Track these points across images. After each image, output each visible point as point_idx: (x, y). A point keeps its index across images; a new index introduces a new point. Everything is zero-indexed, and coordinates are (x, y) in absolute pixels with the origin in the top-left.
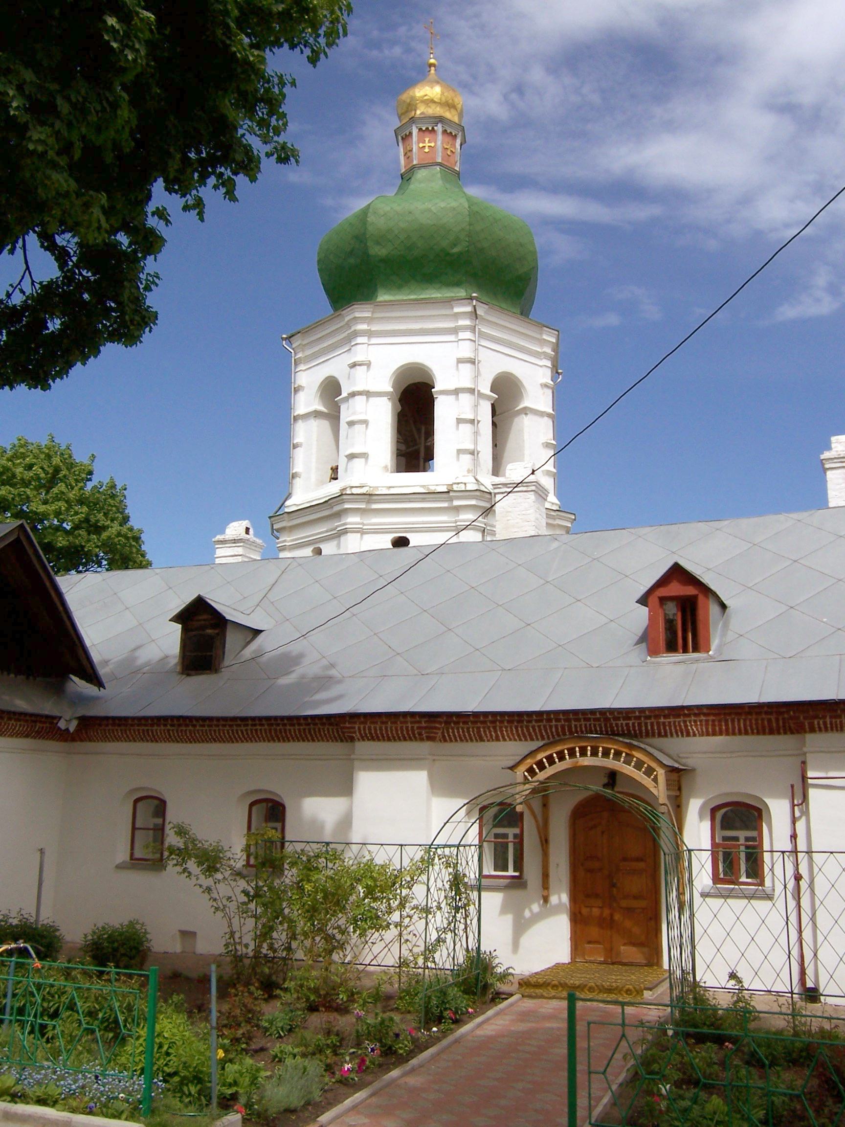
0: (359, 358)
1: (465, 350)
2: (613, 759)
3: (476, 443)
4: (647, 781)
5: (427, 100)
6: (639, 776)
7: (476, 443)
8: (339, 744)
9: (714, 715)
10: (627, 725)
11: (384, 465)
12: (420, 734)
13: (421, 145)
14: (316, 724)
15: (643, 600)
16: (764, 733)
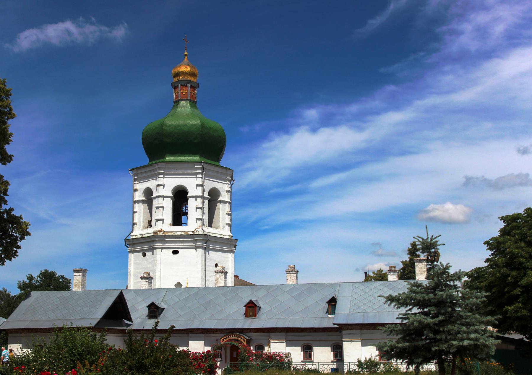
1: (199, 181)
4: (243, 341)
5: (185, 72)
6: (242, 340)
11: (169, 223)
13: (182, 91)
15: (244, 307)
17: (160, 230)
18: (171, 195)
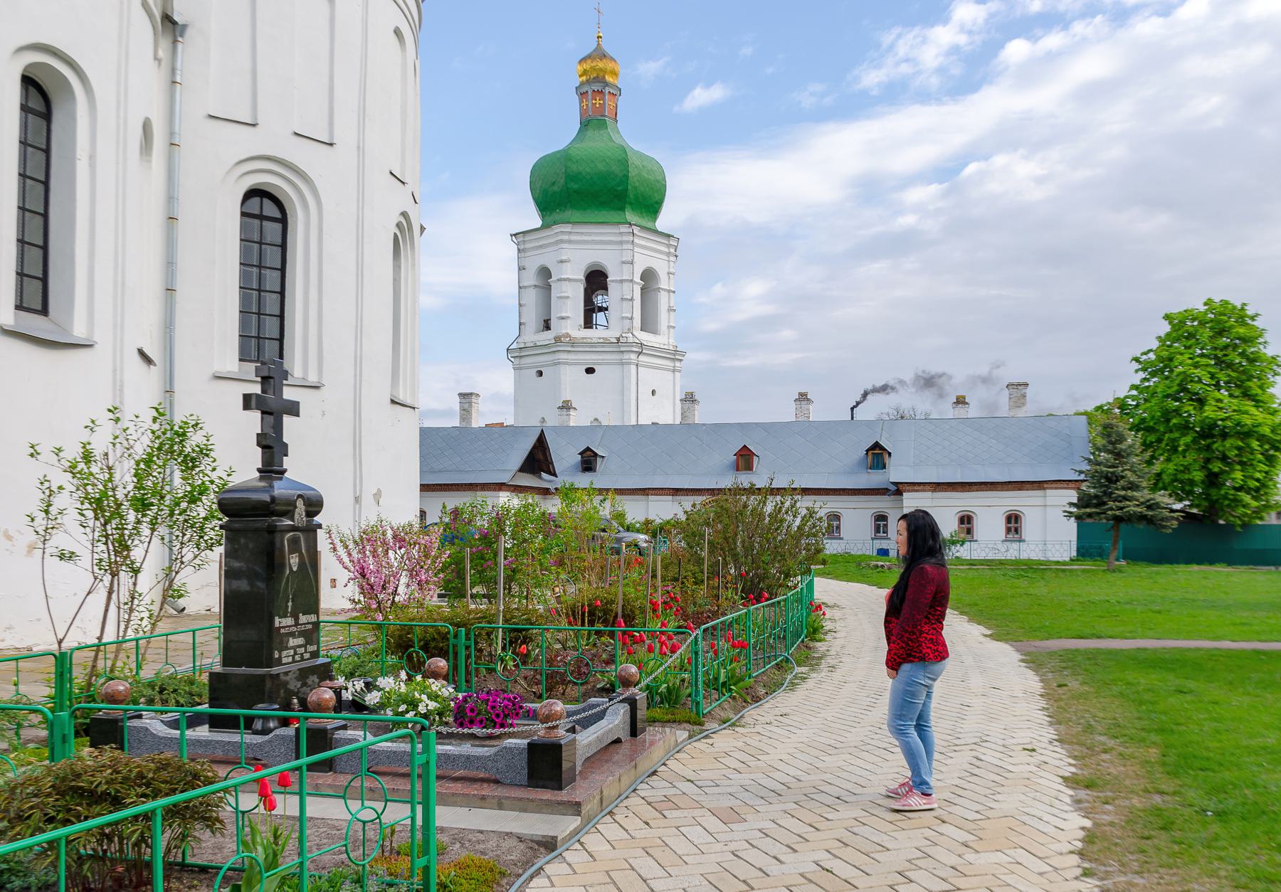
0: (564, 258)
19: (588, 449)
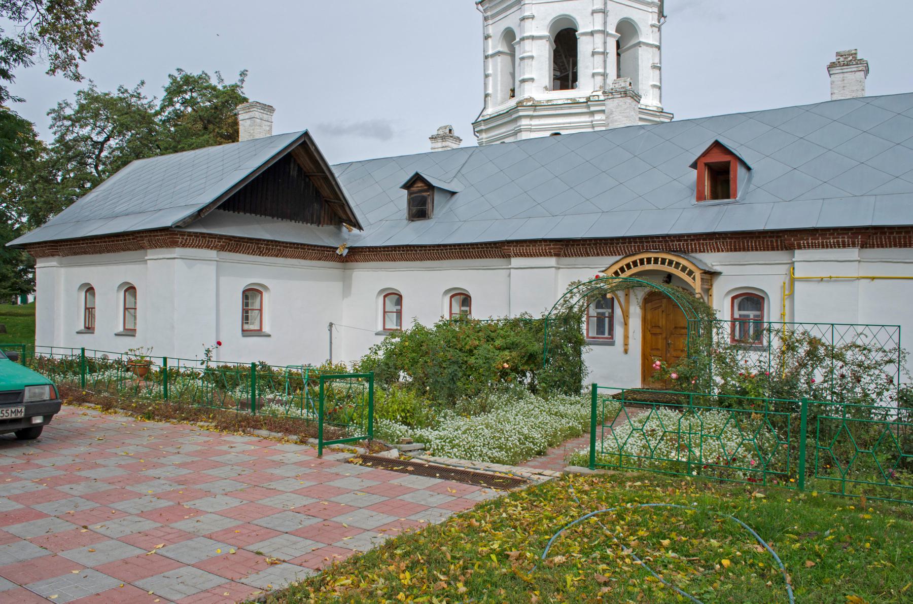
0: (527, 14)
2: (675, 267)
3: (605, 68)
6: (684, 276)
7: (605, 68)
8: (502, 259)
9: (736, 238)
10: (679, 245)
11: (544, 86)
12: (550, 252)
14: (487, 248)
15: (694, 165)
16: (768, 250)
17: (527, 99)
18: (546, 33)
19: (417, 178)
